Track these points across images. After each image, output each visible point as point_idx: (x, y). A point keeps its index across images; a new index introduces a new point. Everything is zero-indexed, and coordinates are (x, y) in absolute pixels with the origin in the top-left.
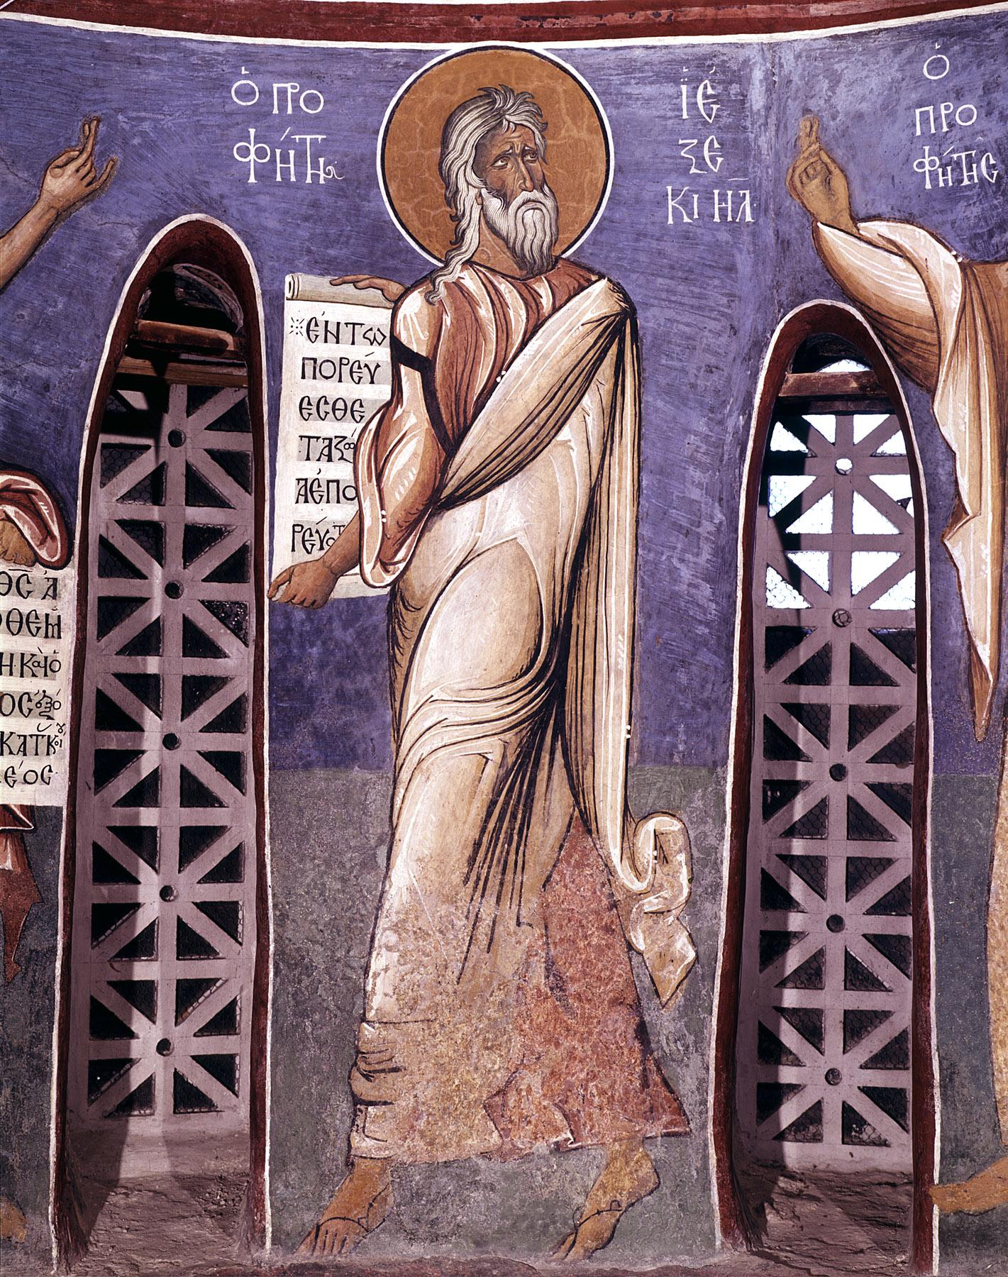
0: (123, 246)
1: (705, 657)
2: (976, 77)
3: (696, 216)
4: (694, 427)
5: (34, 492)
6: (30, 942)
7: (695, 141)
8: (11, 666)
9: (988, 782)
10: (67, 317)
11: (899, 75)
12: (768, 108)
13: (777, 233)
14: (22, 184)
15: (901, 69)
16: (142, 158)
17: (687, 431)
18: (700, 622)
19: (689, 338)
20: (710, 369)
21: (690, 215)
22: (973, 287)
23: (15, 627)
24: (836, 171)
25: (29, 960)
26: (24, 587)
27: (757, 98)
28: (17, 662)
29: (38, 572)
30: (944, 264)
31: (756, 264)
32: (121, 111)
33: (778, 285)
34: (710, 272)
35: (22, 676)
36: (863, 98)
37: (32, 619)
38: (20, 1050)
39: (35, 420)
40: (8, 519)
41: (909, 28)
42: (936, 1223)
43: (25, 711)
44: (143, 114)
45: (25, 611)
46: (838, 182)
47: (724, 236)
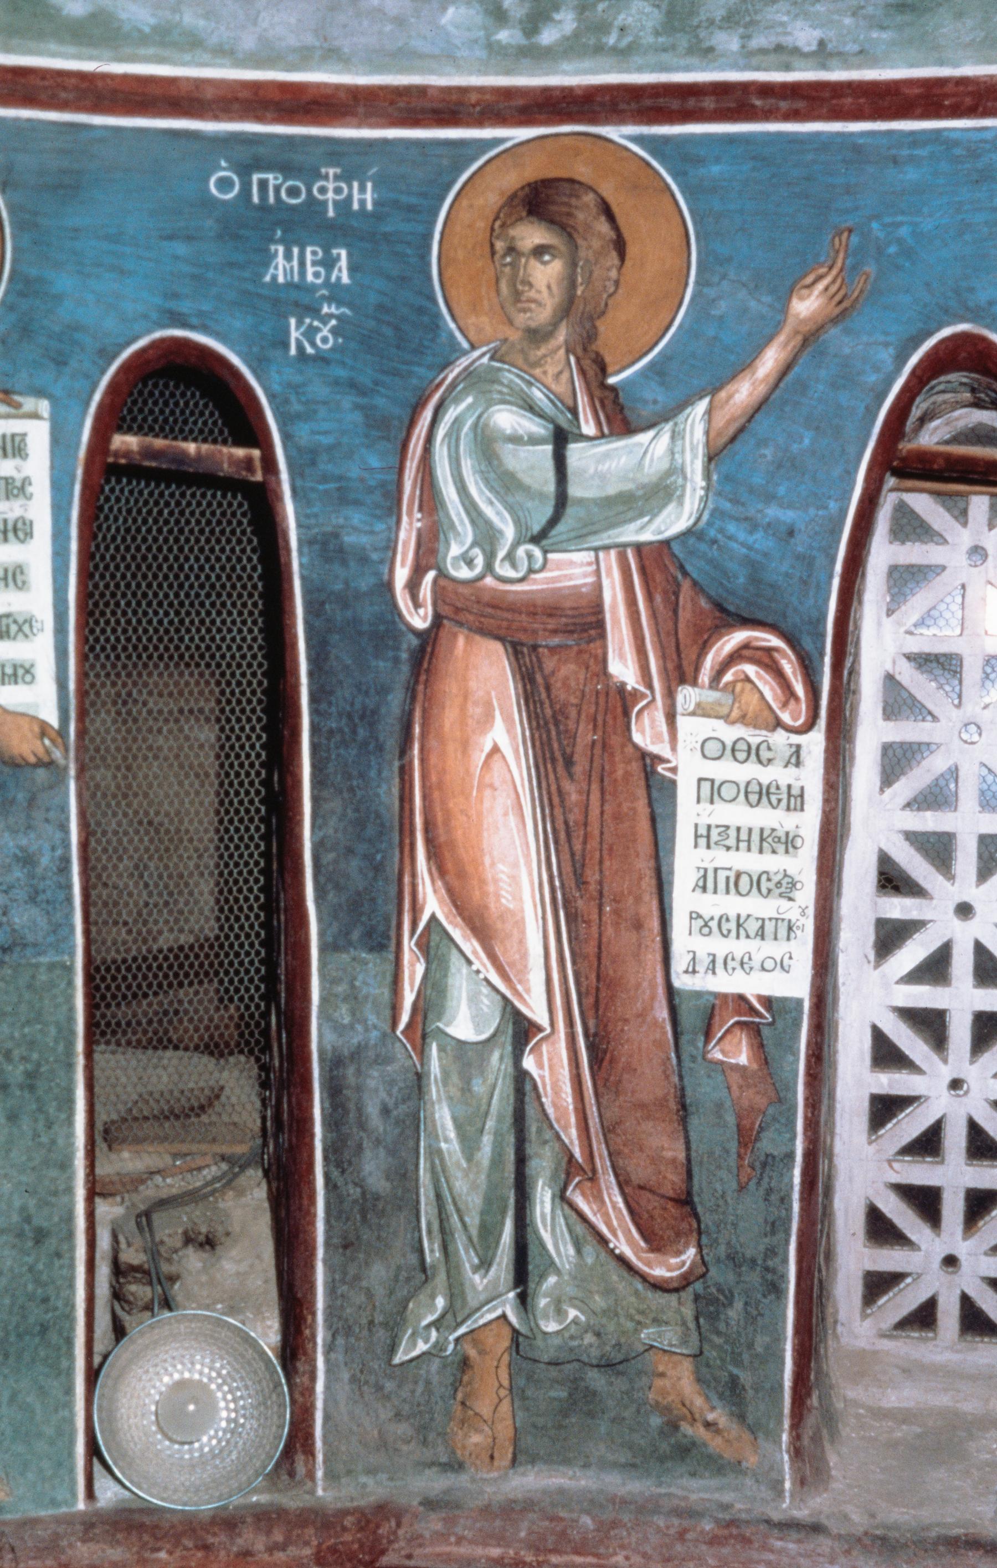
0: (876, 369)
5: (776, 649)
6: (767, 1145)
8: (749, 841)
10: (814, 453)
14: (765, 310)
16: (898, 268)
23: (754, 798)
25: (764, 1165)
26: (765, 754)
28: (756, 837)
29: (780, 739)
32: (877, 217)
35: (761, 851)
37: (773, 790)
38: (753, 1261)
39: (780, 568)
40: (748, 679)
43: (764, 891)
44: (899, 218)
45: (765, 782)
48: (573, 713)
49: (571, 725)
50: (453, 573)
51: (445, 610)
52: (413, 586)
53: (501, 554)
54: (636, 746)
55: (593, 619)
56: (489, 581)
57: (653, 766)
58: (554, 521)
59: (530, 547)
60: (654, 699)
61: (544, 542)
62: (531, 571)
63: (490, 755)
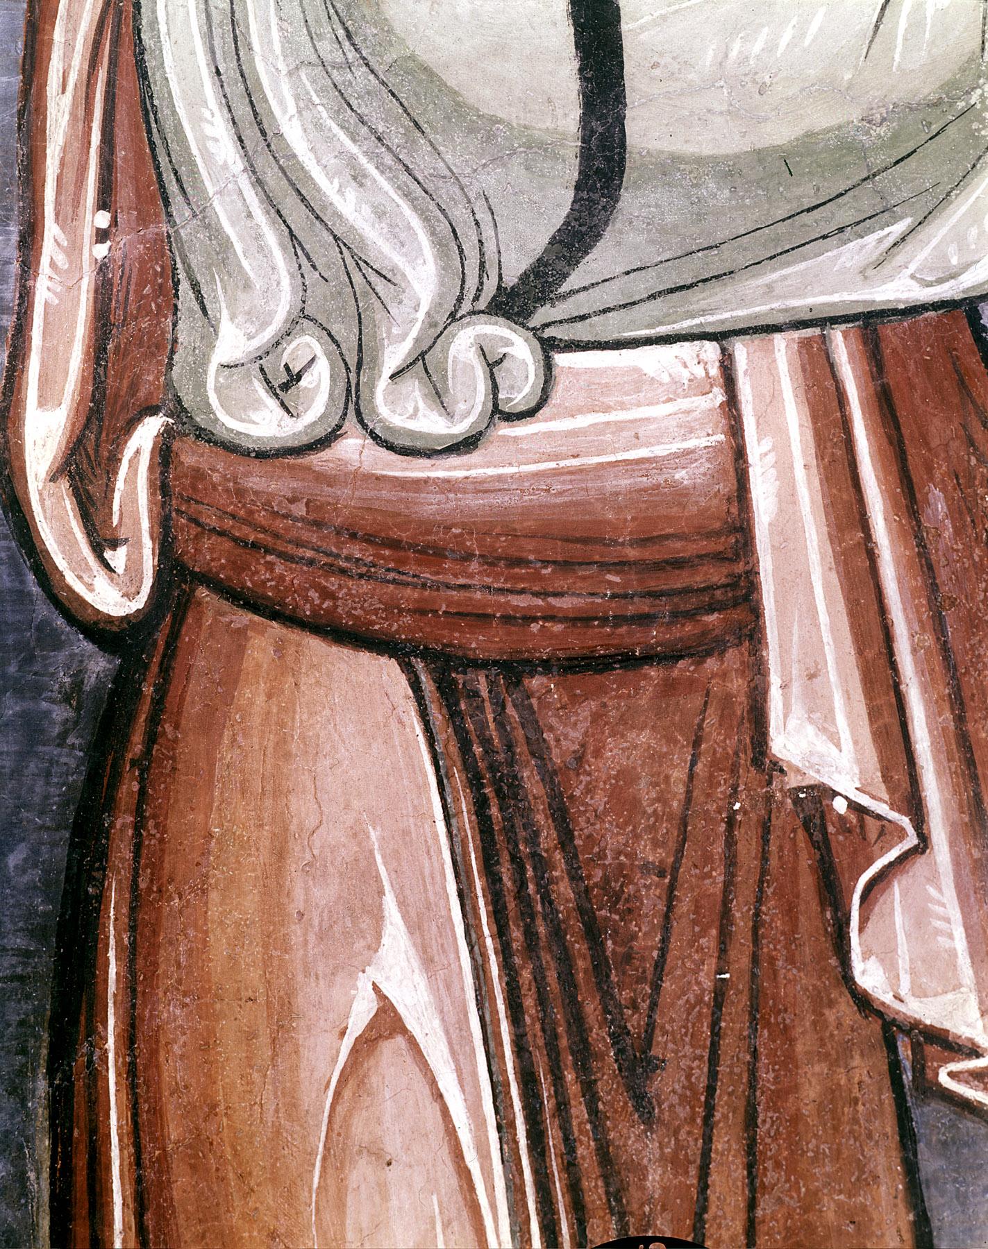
48: (650, 897)
49: (647, 940)
50: (229, 423)
51: (209, 554)
52: (87, 467)
53: (394, 356)
54: (863, 1001)
55: (716, 575)
56: (353, 449)
57: (920, 1069)
58: (576, 238)
59: (497, 330)
60: (924, 842)
61: (543, 314)
62: (499, 413)
63: (367, 1043)
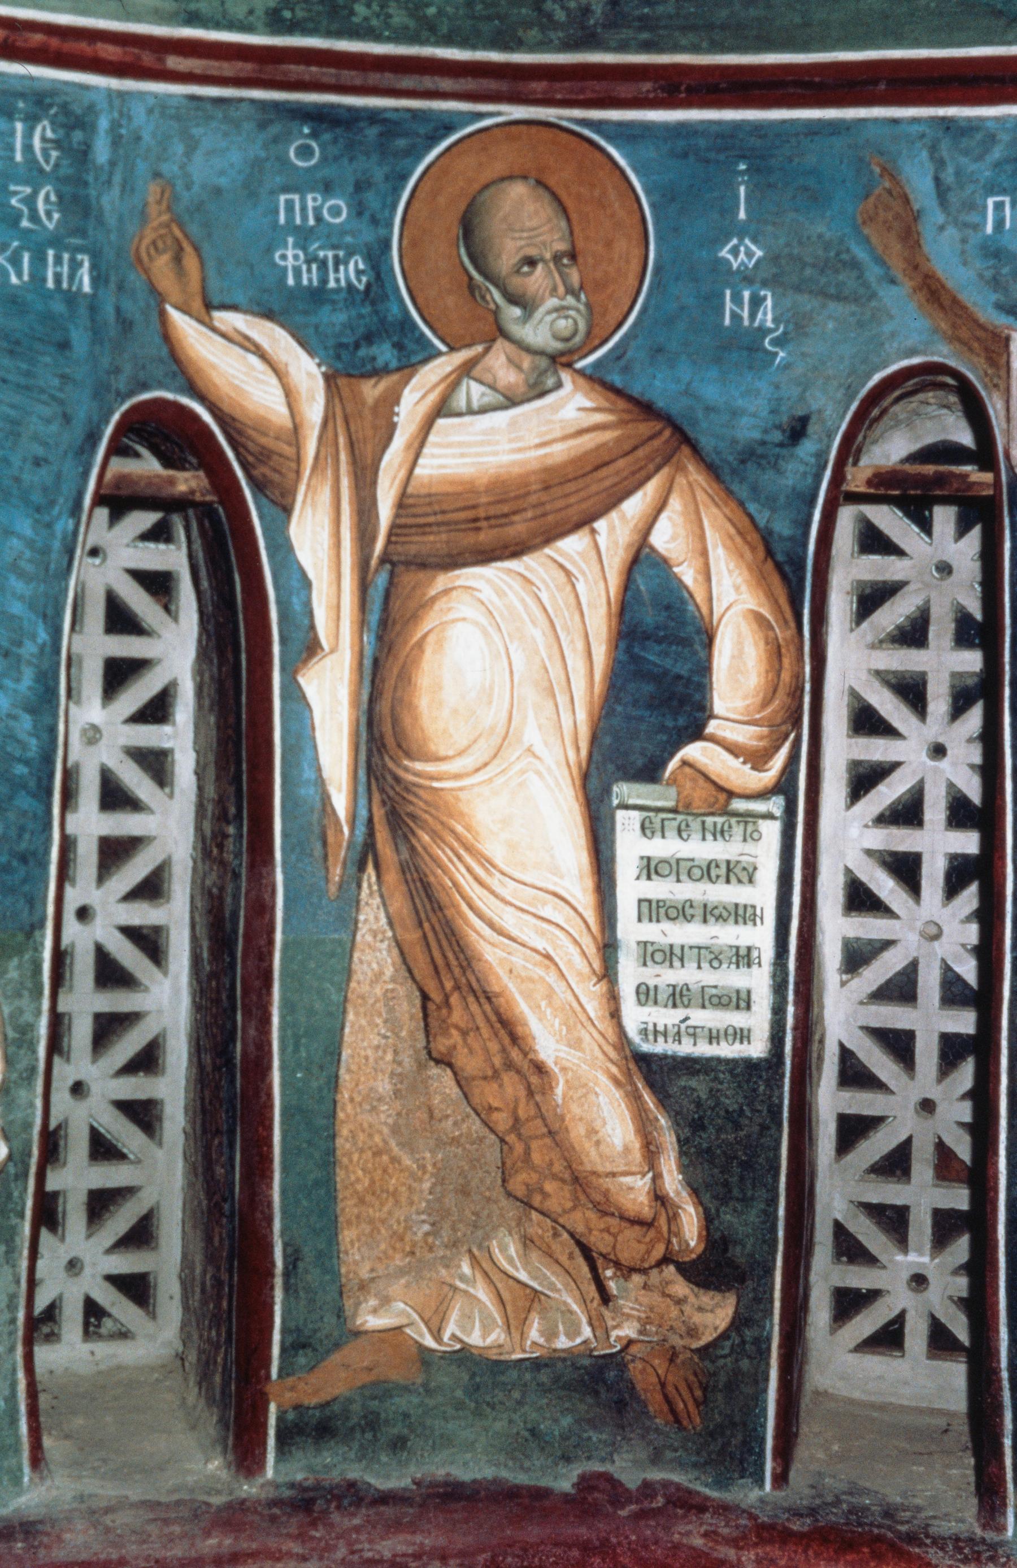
1: (24, 802)
2: (348, 171)
3: (26, 278)
4: (18, 528)
7: (28, 190)
9: (340, 942)
11: (263, 154)
12: (113, 163)
13: (118, 310)
15: (265, 146)
17: (9, 533)
18: (20, 760)
19: (15, 422)
20: (38, 462)
21: (19, 274)
22: (337, 401)
24: (188, 249)
27: (102, 152)
30: (307, 371)
31: (93, 343)
33: (117, 371)
34: (38, 346)
36: (222, 173)
41: (276, 105)
42: (272, 1421)
46: (191, 262)
47: (58, 307)
